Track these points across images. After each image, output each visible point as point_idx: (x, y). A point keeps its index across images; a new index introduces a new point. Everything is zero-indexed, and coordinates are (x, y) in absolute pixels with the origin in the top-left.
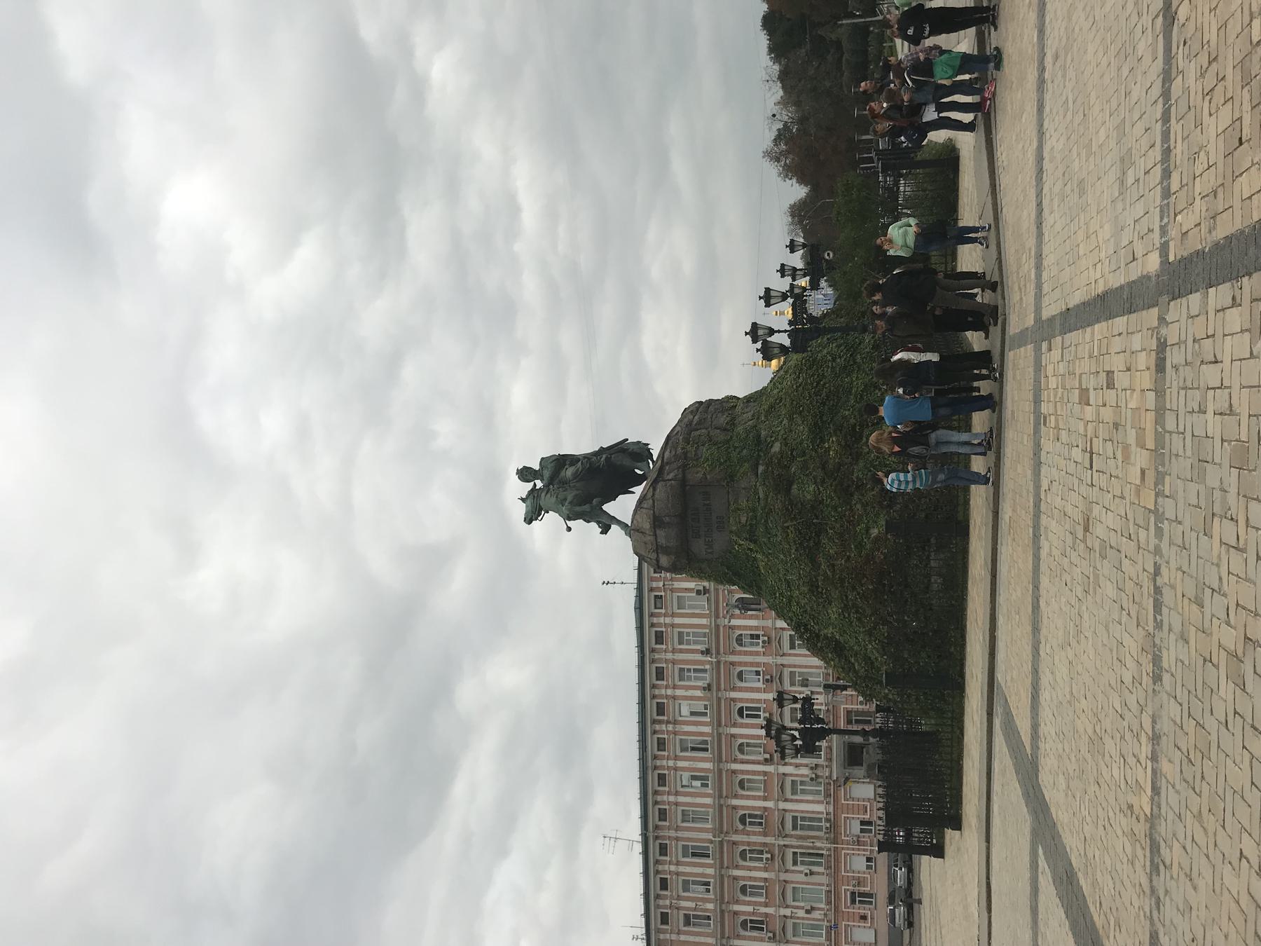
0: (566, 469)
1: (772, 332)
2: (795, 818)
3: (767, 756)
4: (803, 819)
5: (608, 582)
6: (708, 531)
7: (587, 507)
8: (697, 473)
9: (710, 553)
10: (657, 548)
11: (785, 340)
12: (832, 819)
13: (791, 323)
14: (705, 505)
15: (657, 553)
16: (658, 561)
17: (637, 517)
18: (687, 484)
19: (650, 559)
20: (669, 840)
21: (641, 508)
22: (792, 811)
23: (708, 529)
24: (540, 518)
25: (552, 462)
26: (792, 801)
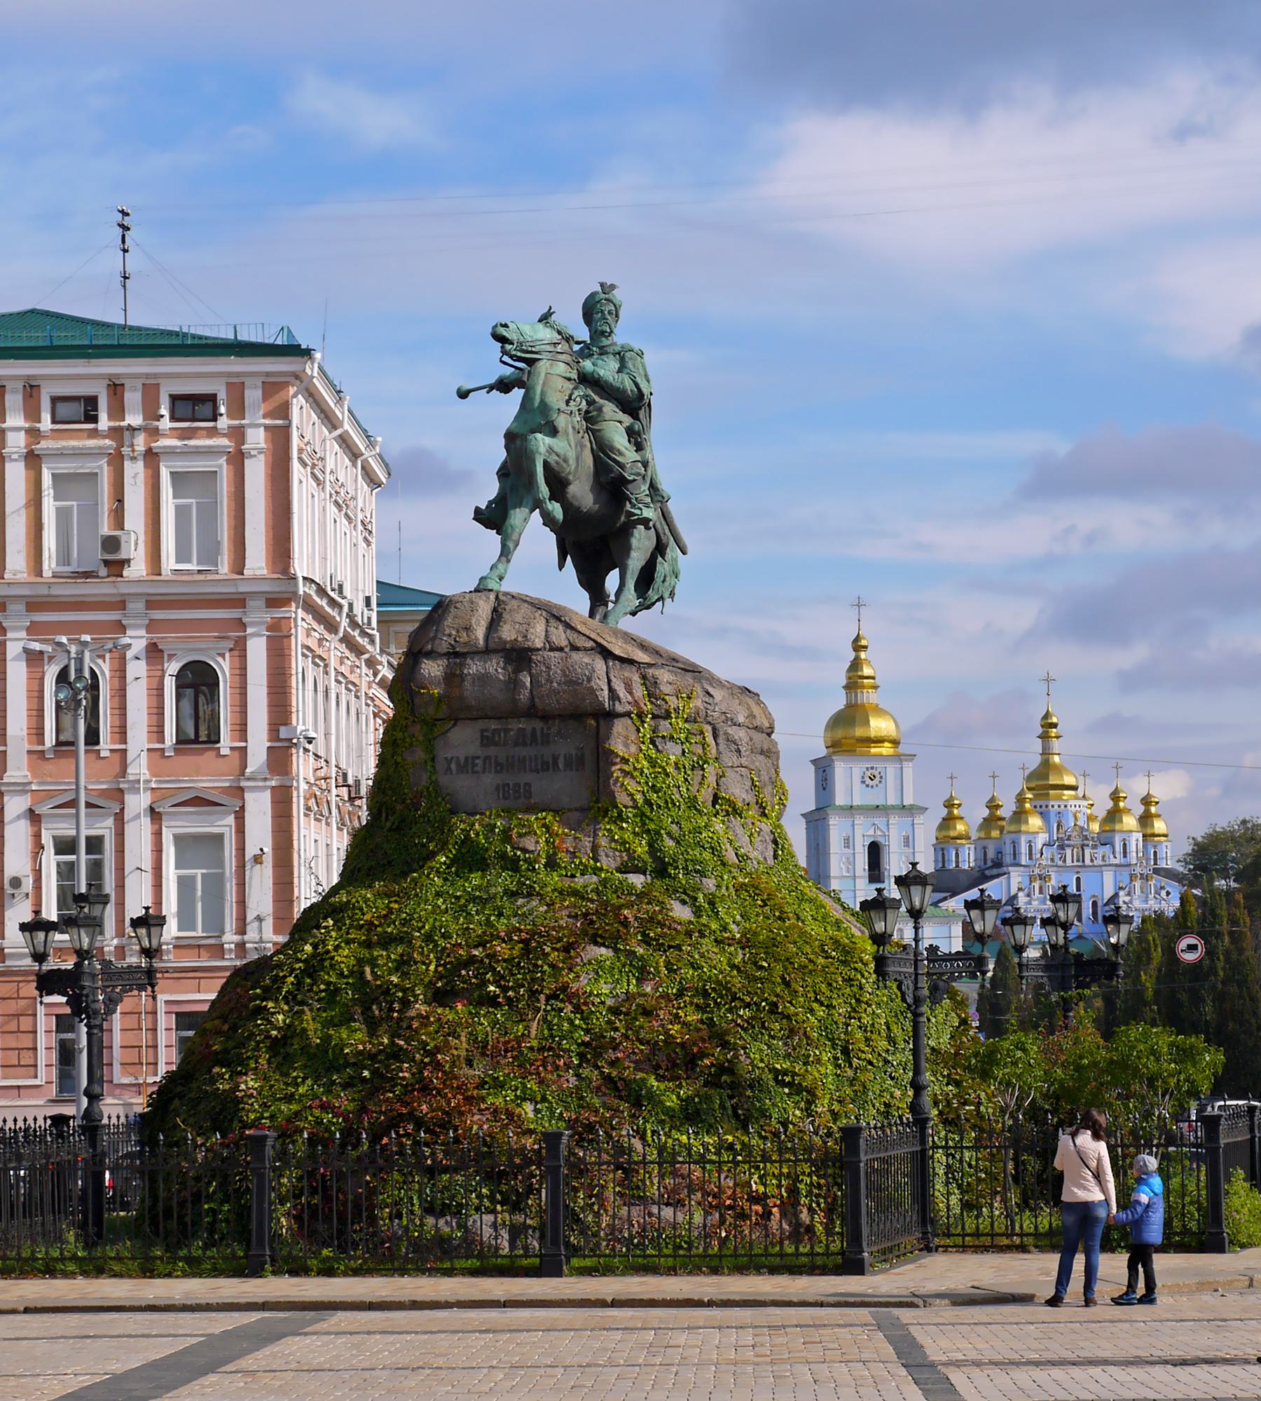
0: (620, 422)
5: (128, 229)
6: (497, 764)
9: (449, 769)
10: (456, 655)
13: (933, 949)
14: (555, 759)
15: (448, 655)
16: (431, 655)
17: (525, 608)
18: (602, 722)
19: (435, 638)
21: (547, 621)
23: (501, 765)
24: (506, 359)
25: (637, 385)
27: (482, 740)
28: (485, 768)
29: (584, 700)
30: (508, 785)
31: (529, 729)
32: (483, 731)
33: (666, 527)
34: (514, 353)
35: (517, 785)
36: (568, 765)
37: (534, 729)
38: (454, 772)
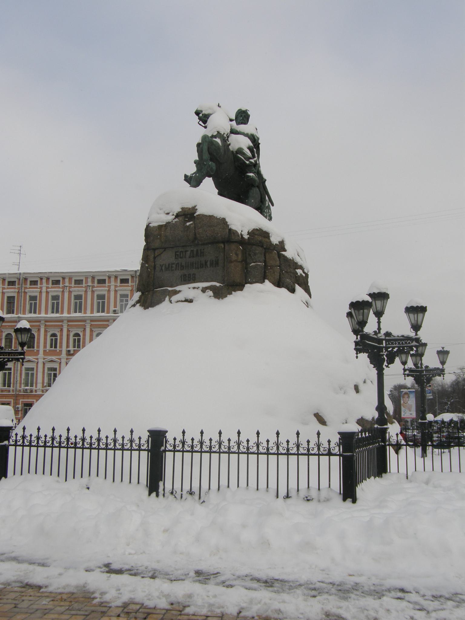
1: (379, 314)
2: (32, 369)
3: (72, 352)
4: (32, 374)
6: (182, 266)
7: (206, 156)
8: (237, 255)
9: (162, 269)
11: (370, 328)
12: (32, 394)
14: (206, 262)
20: (18, 287)
22: (37, 367)
24: (201, 123)
26: (44, 367)
27: (175, 256)
28: (176, 268)
29: (218, 233)
30: (186, 275)
31: (195, 250)
32: (176, 252)
33: (264, 192)
34: (203, 118)
35: (189, 275)
36: (211, 264)
37: (197, 250)
38: (164, 270)
